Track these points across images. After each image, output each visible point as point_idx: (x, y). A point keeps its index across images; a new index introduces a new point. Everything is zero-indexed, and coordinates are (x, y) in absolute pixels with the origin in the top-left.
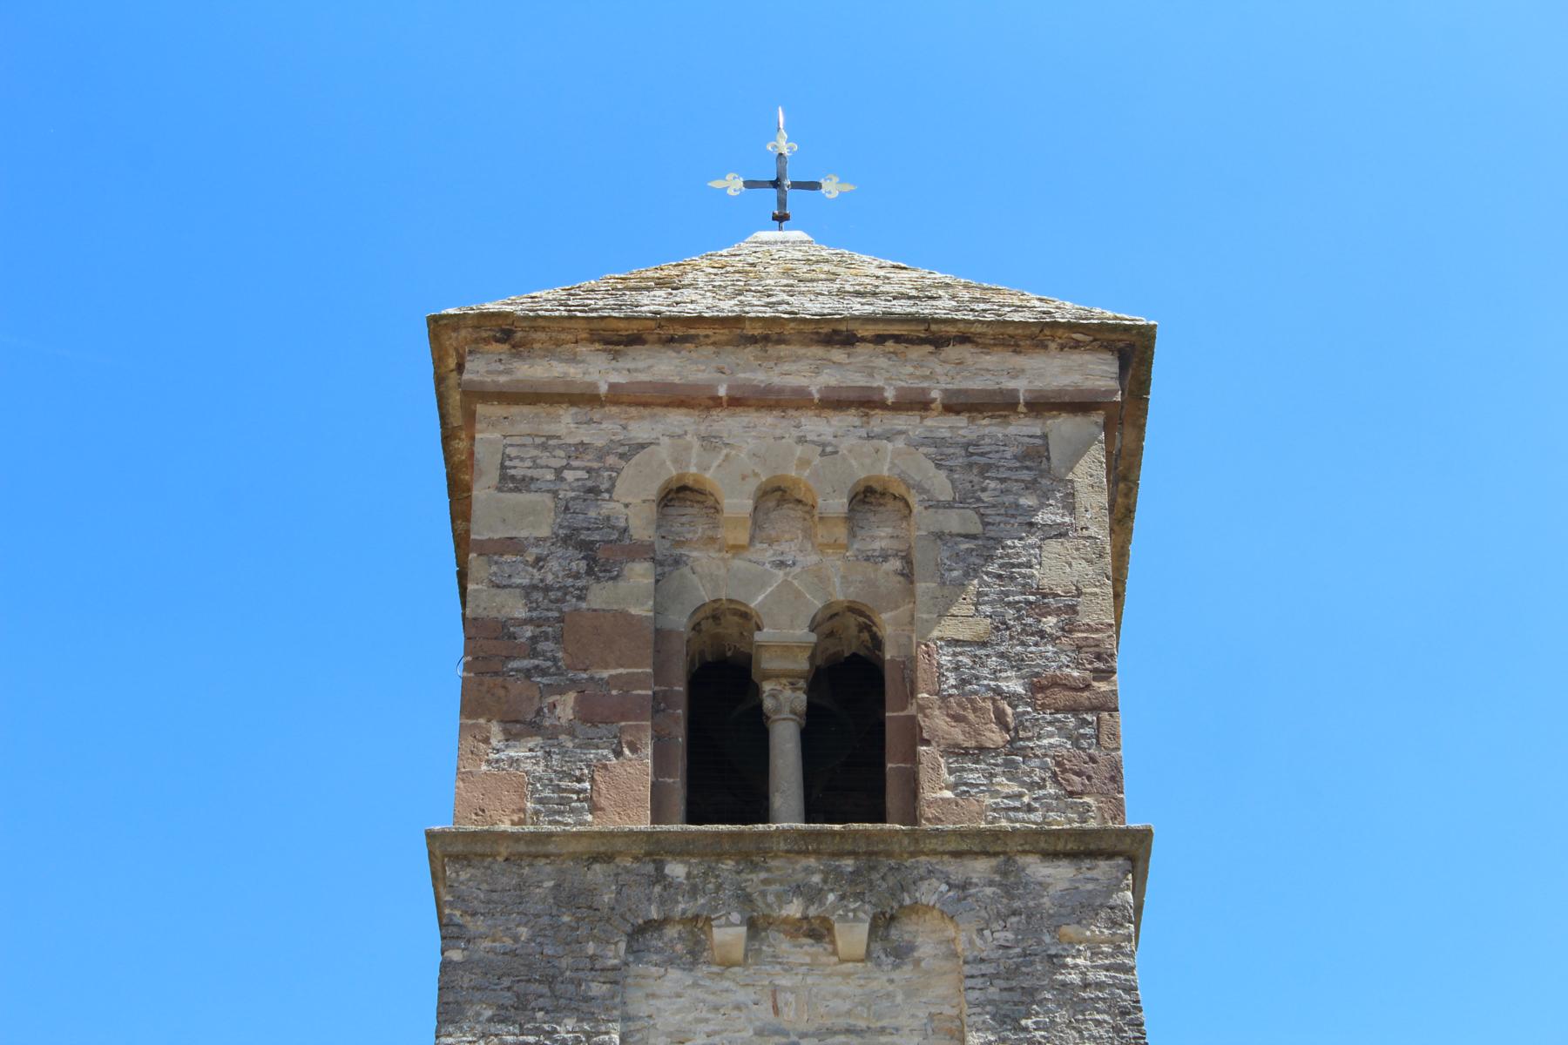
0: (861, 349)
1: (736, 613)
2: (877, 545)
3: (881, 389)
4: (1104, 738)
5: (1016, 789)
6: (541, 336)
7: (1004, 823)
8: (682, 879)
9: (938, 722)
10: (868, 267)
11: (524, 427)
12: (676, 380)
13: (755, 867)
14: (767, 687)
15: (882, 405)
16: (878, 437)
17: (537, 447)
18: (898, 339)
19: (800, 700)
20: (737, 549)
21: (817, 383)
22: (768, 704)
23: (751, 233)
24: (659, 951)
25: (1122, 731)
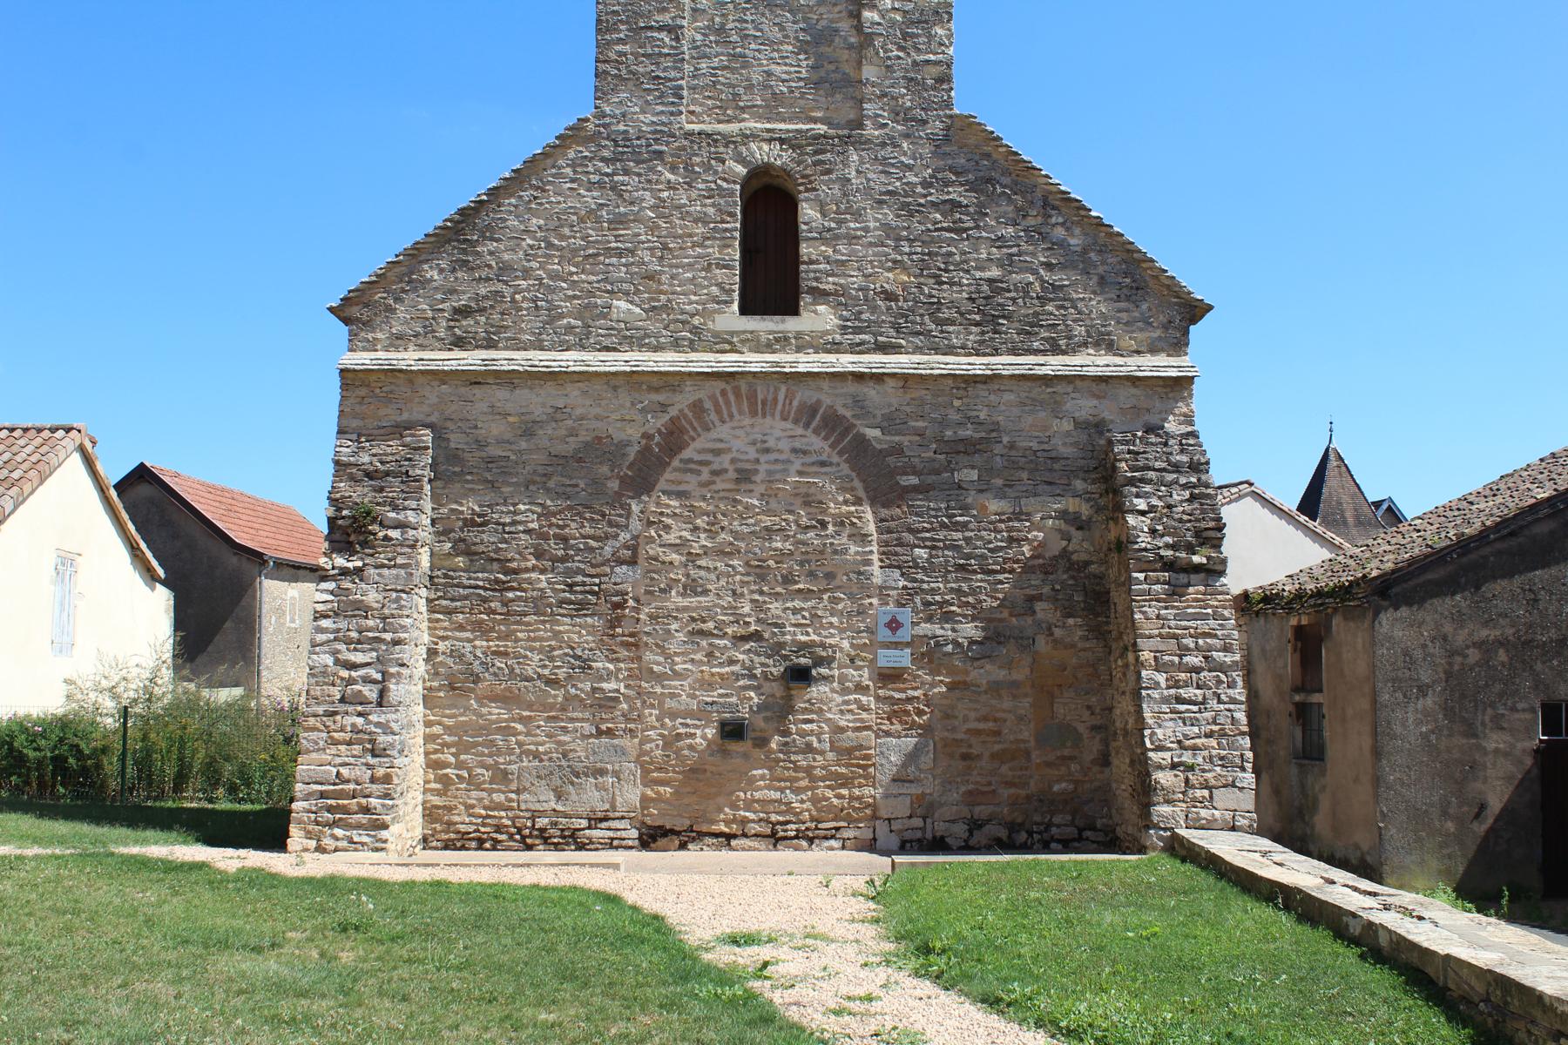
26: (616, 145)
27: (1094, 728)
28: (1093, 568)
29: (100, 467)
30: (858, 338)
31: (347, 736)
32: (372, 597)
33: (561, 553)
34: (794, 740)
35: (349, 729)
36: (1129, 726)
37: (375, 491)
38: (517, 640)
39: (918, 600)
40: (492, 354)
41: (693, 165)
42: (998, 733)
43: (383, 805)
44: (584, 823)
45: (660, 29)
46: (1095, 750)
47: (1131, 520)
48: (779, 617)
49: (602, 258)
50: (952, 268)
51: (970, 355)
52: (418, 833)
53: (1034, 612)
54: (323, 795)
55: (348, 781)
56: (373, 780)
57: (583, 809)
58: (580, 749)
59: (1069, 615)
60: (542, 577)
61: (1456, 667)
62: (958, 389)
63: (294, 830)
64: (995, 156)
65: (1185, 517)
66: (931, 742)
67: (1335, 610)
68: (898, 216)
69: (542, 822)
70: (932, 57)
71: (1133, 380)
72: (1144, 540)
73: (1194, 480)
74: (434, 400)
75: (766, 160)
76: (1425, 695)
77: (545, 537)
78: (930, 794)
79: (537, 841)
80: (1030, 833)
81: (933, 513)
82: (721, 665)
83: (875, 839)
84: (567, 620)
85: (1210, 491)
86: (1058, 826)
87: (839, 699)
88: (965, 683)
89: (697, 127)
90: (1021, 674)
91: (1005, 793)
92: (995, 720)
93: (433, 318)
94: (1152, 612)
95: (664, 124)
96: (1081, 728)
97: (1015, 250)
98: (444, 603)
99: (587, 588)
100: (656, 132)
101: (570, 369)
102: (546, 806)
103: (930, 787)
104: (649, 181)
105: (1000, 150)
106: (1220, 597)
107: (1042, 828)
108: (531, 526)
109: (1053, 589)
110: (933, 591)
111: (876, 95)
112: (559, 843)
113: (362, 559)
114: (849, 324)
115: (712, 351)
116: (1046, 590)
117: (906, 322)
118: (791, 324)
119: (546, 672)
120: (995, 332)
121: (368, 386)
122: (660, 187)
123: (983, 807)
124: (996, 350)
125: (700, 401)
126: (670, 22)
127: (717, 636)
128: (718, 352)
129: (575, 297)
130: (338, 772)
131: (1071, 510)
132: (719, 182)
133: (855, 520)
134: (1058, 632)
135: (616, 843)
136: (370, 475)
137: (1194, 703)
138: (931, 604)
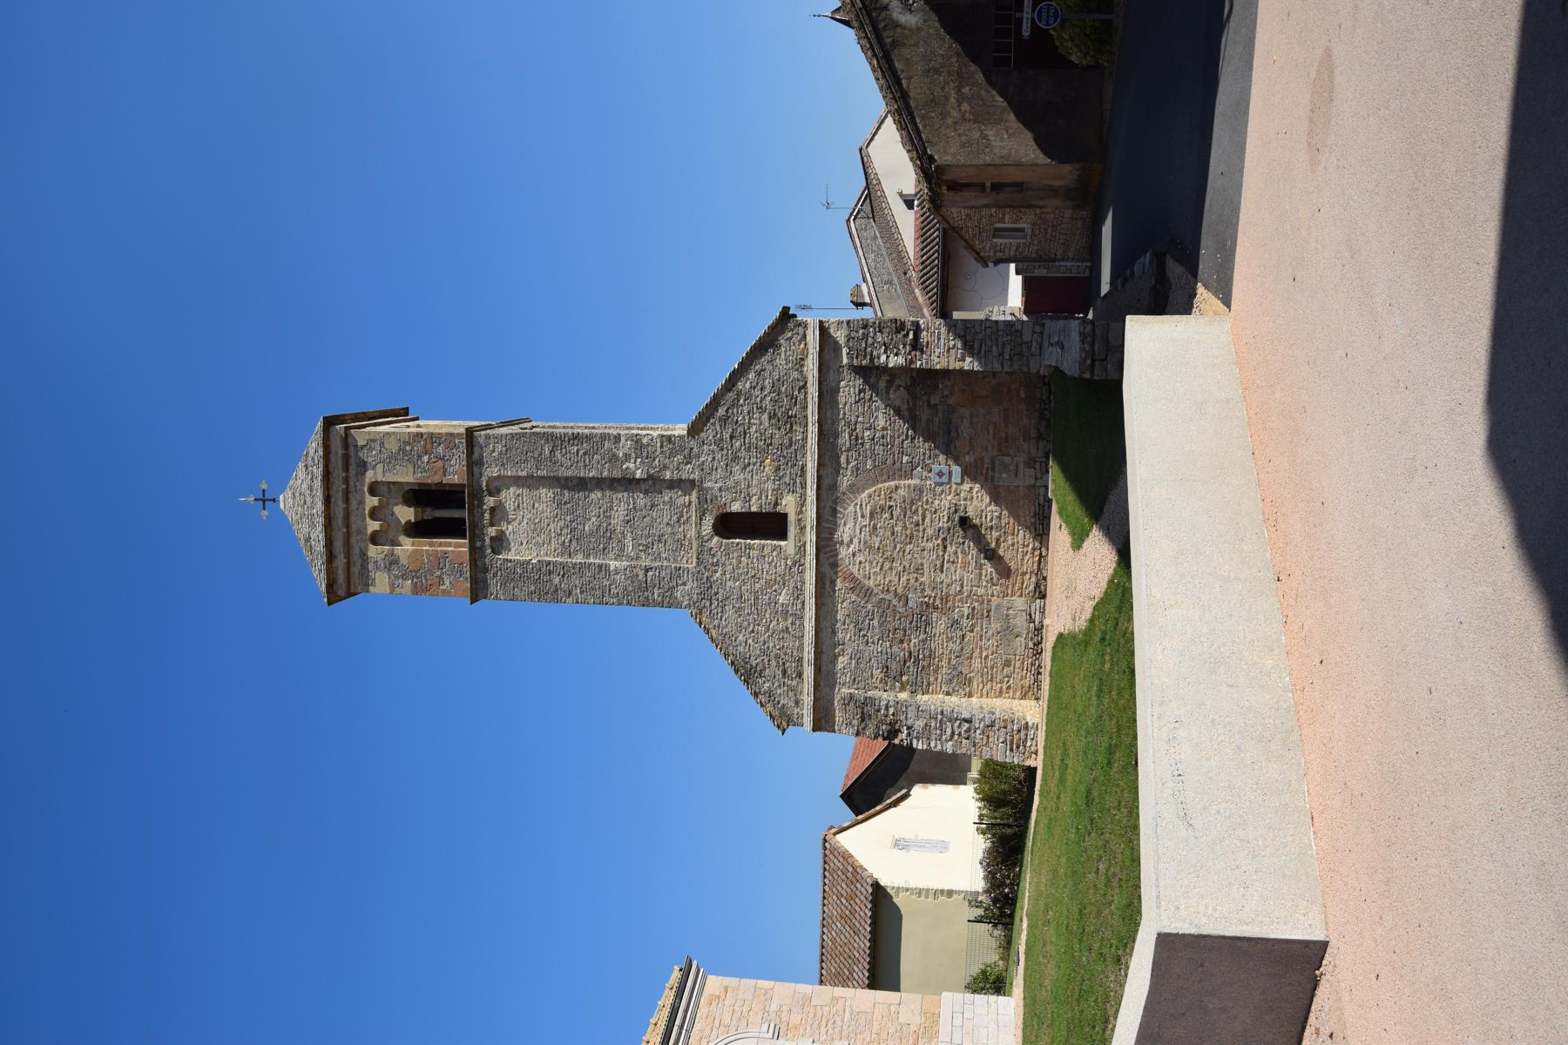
0: (332, 493)
2: (386, 489)
9: (436, 479)
11: (357, 580)
14: (425, 518)
20: (389, 525)
21: (342, 506)
22: (430, 518)
23: (282, 511)
28: (914, 374)
29: (845, 825)
30: (798, 485)
31: (985, 738)
33: (902, 632)
38: (943, 653)
39: (927, 462)
40: (806, 660)
42: (995, 424)
44: (1032, 625)
45: (646, 576)
47: (891, 365)
48: (935, 530)
49: (759, 607)
50: (763, 438)
52: (1033, 703)
53: (936, 405)
54: (1011, 750)
55: (1006, 738)
56: (1005, 728)
57: (1025, 624)
58: (995, 626)
60: (913, 641)
61: (972, 117)
63: (1027, 763)
65: (890, 337)
69: (1031, 645)
70: (658, 445)
73: (871, 330)
76: (987, 135)
77: (894, 638)
82: (958, 558)
85: (877, 322)
87: (975, 502)
89: (695, 561)
91: (1025, 421)
92: (989, 425)
94: (937, 360)
97: (755, 406)
103: (1021, 458)
106: (930, 325)
108: (888, 646)
110: (924, 454)
115: (804, 556)
116: (925, 398)
118: (792, 518)
120: (796, 417)
122: (724, 578)
125: (829, 564)
127: (944, 559)
129: (778, 620)
134: (946, 393)
136: (863, 719)
138: (930, 456)
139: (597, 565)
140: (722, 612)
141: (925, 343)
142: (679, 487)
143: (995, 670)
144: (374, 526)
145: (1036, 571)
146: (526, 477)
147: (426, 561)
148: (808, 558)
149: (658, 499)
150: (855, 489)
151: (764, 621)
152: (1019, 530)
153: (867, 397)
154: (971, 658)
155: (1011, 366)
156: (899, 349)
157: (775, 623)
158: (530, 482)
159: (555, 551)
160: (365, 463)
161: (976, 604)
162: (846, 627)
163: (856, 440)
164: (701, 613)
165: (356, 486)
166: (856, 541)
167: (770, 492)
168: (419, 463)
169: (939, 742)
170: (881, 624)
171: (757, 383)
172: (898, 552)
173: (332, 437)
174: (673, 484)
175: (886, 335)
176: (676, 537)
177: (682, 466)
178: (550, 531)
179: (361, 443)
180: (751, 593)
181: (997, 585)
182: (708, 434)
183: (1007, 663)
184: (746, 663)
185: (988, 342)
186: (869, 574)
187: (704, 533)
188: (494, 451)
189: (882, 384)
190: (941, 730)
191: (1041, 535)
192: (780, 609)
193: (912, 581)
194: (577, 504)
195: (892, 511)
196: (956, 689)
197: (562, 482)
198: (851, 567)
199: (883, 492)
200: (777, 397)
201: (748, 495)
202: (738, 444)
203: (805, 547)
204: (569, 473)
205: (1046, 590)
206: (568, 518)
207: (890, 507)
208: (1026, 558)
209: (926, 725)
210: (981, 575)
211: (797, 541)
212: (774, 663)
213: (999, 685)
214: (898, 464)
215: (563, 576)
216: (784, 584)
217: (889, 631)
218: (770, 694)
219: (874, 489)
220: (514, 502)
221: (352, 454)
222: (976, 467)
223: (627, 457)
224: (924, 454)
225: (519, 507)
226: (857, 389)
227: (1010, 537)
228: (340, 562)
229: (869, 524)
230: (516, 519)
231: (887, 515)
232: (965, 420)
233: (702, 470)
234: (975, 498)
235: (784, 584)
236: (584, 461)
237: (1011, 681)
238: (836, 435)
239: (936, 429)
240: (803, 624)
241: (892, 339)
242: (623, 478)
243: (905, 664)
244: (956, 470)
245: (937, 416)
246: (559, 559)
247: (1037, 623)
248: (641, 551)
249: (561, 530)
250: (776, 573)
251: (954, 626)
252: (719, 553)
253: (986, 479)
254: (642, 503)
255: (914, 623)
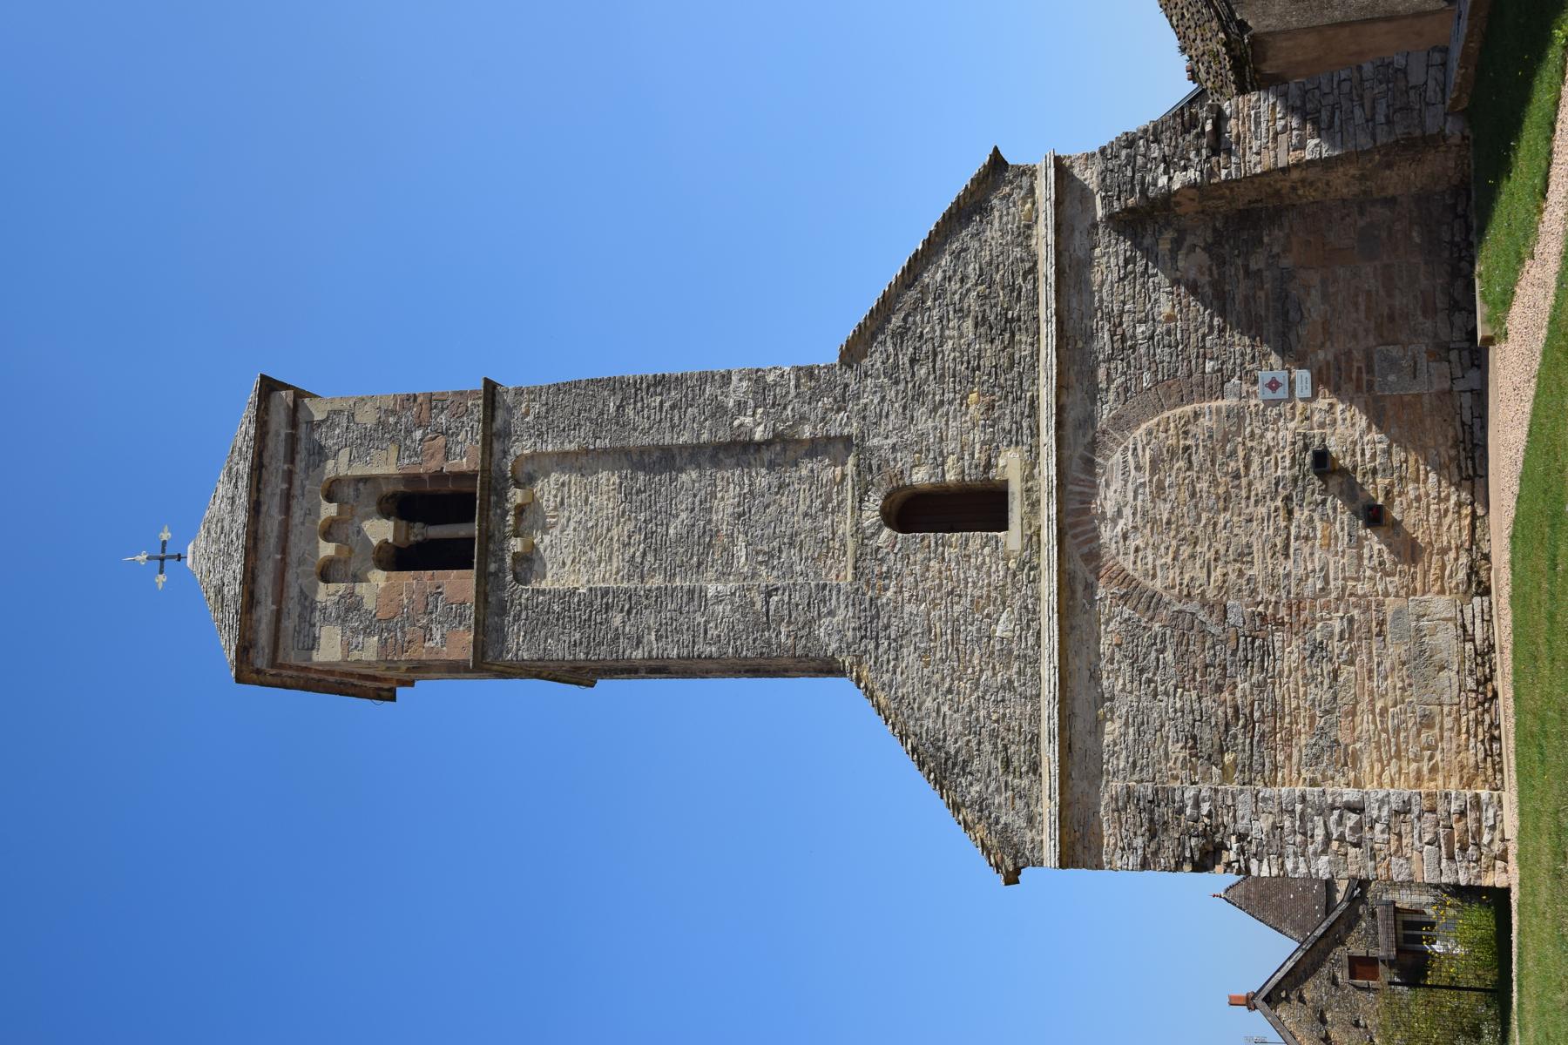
0: (262, 499)
1: (379, 552)
2: (352, 493)
3: (282, 490)
4: (443, 398)
5: (464, 432)
6: (247, 634)
7: (478, 437)
8: (497, 565)
9: (433, 465)
10: (218, 506)
11: (290, 642)
12: (272, 576)
13: (494, 535)
14: (412, 539)
15: (289, 489)
16: (303, 492)
17: (299, 636)
18: (259, 482)
19: (419, 525)
20: (351, 551)
22: (420, 538)
24: (526, 574)
25: (441, 391)
26: (865, 637)
27: (1362, 213)
30: (1026, 431)
31: (1394, 838)
32: (1264, 823)
33: (1218, 671)
34: (1381, 464)
35: (1386, 836)
36: (1357, 173)
37: (1166, 830)
38: (1298, 707)
39: (1249, 367)
41: (882, 573)
42: (1369, 293)
43: (1457, 798)
44: (1469, 646)
45: (768, 603)
46: (1381, 211)
47: (1176, 186)
48: (1269, 482)
49: (960, 647)
50: (966, 358)
51: (1038, 339)
53: (1259, 270)
54: (1451, 857)
55: (1436, 834)
56: (1433, 810)
57: (1455, 646)
59: (1261, 241)
60: (1240, 686)
62: (1068, 344)
63: (1487, 881)
64: (874, 328)
66: (1379, 348)
67: (1256, 71)
68: (924, 403)
69: (1471, 683)
70: (793, 383)
71: (1058, 204)
72: (1192, 174)
74: (1085, 784)
75: (877, 513)
78: (1427, 345)
79: (1489, 687)
80: (1461, 259)
81: (1174, 358)
82: (1314, 529)
83: (1472, 391)
84: (1279, 663)
86: (1453, 235)
87: (1340, 429)
88: (1323, 323)
89: (850, 571)
90: (1315, 278)
92: (1357, 296)
93: (1013, 790)
94: (1255, 158)
95: (848, 598)
96: (1361, 223)
97: (951, 308)
98: (1267, 773)
99: (1249, 647)
100: (854, 605)
101: (1056, 664)
102: (1455, 679)
104: (895, 609)
105: (868, 324)
107: (1455, 249)
108: (1194, 697)
109: (1238, 256)
110: (1243, 355)
111: (824, 426)
112: (1490, 667)
113: (1229, 836)
114: (1014, 439)
115: (1039, 552)
116: (1239, 262)
117: (1012, 393)
118: (1015, 488)
119: (1326, 682)
120: (1019, 320)
121: (1073, 843)
122: (900, 599)
123: (1437, 301)
124: (1034, 318)
125: (1082, 556)
126: (762, 596)
127: (1289, 534)
128: (1039, 547)
129: (994, 668)
130: (1428, 844)
131: (1169, 247)
132: (896, 551)
133: (1182, 422)
134: (1276, 250)
135: (1486, 617)
136: (1153, 835)
137: (1333, 114)
138: (1253, 357)
139: (685, 589)
140: (896, 659)
141: (1232, 140)
142: (825, 453)
143: (1402, 735)
144: (327, 549)
145: (1467, 545)
146: (576, 454)
147: (406, 601)
148: (1044, 553)
149: (790, 475)
150: (1122, 423)
151: (970, 670)
152: (1427, 474)
153: (1139, 269)
154: (1354, 714)
155: (1390, 133)
156: (1189, 160)
157: (990, 673)
158: (581, 461)
159: (617, 573)
160: (321, 448)
161: (1355, 613)
162: (1116, 666)
163: (1124, 343)
164: (859, 664)
165: (303, 487)
166: (1127, 511)
167: (978, 446)
168: (408, 442)
169: (1301, 859)
170: (1179, 659)
171: (955, 271)
172: (1205, 526)
173: (272, 408)
174: (818, 447)
175: (1166, 142)
176: (820, 536)
177: (830, 415)
178: (611, 539)
179: (318, 417)
180: (947, 621)
181: (1394, 575)
182: (875, 360)
183: (1427, 721)
184: (939, 749)
185: (1345, 104)
186: (1154, 568)
187: (866, 524)
188: (527, 414)
189: (1164, 246)
190: (1304, 834)
191: (1469, 478)
192: (998, 647)
193: (1232, 577)
194: (658, 492)
195: (1190, 455)
196: (1329, 773)
197: (635, 458)
198: (1120, 558)
199: (1172, 425)
200: (988, 291)
201: (941, 453)
202: (923, 371)
203: (1039, 536)
204: (647, 440)
205: (1489, 579)
206: (642, 517)
207: (1186, 448)
208: (1447, 521)
209: (1274, 827)
210: (1360, 557)
211: (1026, 527)
212: (987, 747)
213: (1414, 766)
214: (1196, 376)
215: (629, 612)
216: (1004, 603)
217: (1195, 670)
218: (982, 805)
219: (1156, 420)
220: (556, 496)
221: (303, 436)
222: (1339, 369)
223: (741, 407)
224: (1243, 355)
225: (562, 503)
226: (1121, 258)
227: (1411, 486)
228: (266, 610)
229: (1151, 481)
230: (556, 523)
231: (1181, 463)
232: (1313, 292)
233: (864, 418)
234: (1340, 421)
235: (1004, 603)
236: (671, 420)
237: (1438, 756)
238: (1091, 336)
239: (1263, 313)
240: (1038, 672)
241: (1176, 147)
242: (733, 443)
243: (1227, 731)
244: (1303, 377)
245: (1262, 288)
246: (625, 585)
247: (1478, 642)
248: (761, 563)
249: (630, 537)
250: (989, 585)
251: (1317, 655)
252: (892, 556)
253: (1358, 388)
254: (764, 483)
255: (1240, 653)
